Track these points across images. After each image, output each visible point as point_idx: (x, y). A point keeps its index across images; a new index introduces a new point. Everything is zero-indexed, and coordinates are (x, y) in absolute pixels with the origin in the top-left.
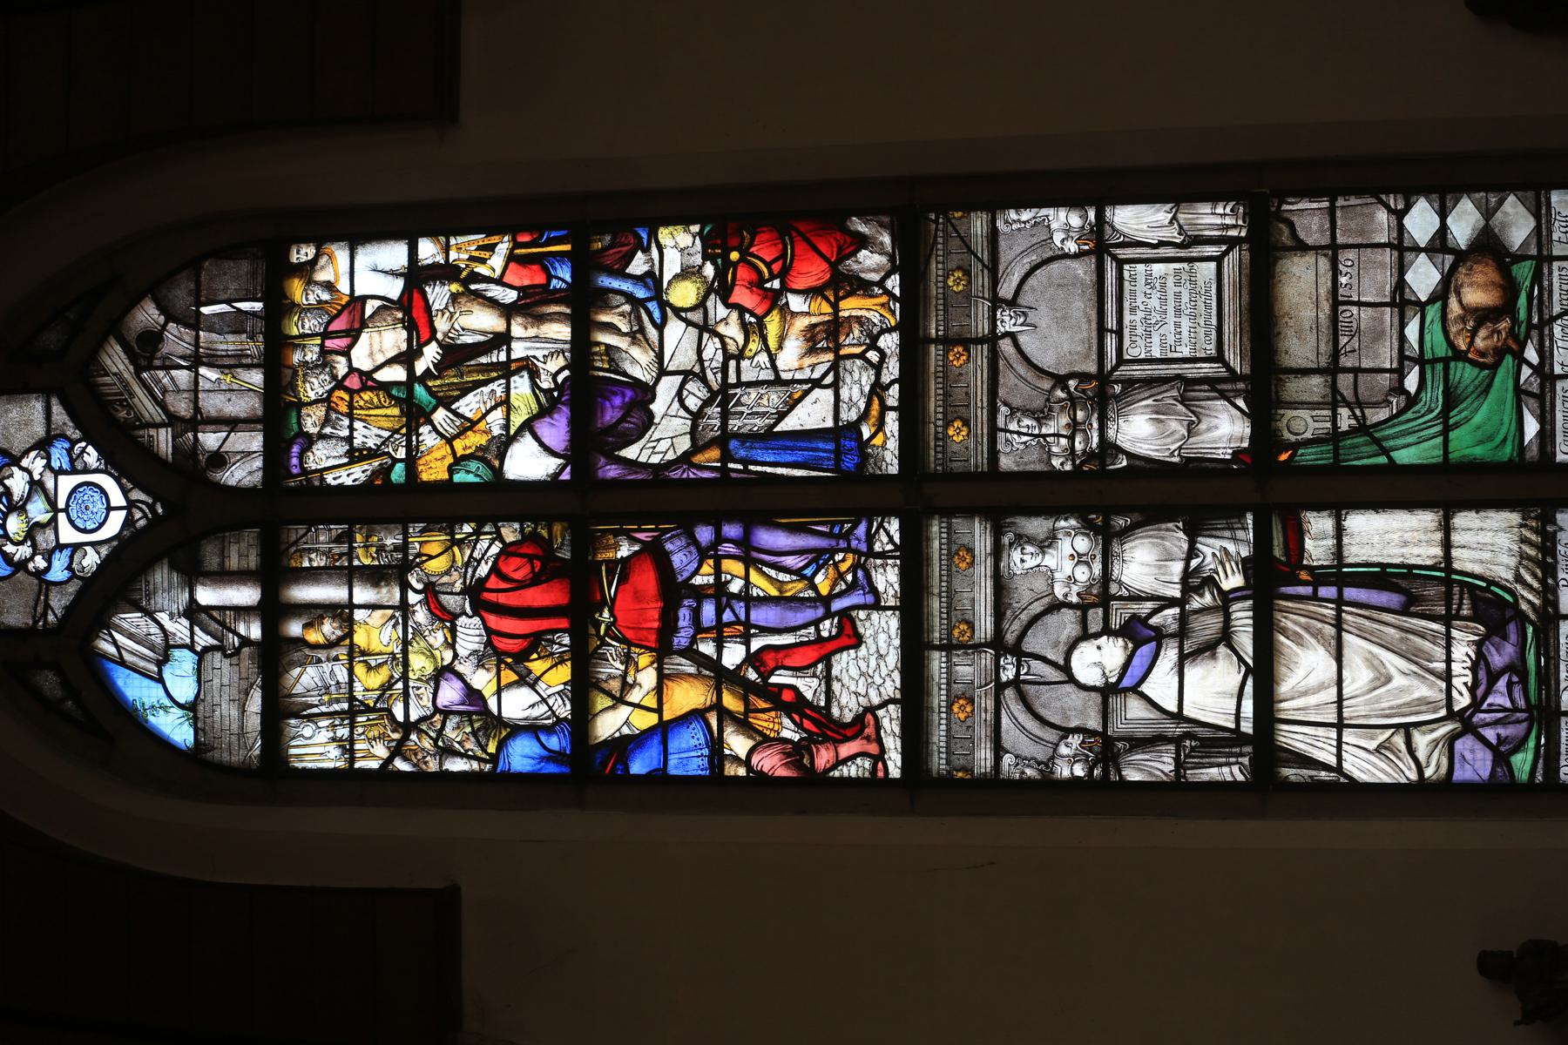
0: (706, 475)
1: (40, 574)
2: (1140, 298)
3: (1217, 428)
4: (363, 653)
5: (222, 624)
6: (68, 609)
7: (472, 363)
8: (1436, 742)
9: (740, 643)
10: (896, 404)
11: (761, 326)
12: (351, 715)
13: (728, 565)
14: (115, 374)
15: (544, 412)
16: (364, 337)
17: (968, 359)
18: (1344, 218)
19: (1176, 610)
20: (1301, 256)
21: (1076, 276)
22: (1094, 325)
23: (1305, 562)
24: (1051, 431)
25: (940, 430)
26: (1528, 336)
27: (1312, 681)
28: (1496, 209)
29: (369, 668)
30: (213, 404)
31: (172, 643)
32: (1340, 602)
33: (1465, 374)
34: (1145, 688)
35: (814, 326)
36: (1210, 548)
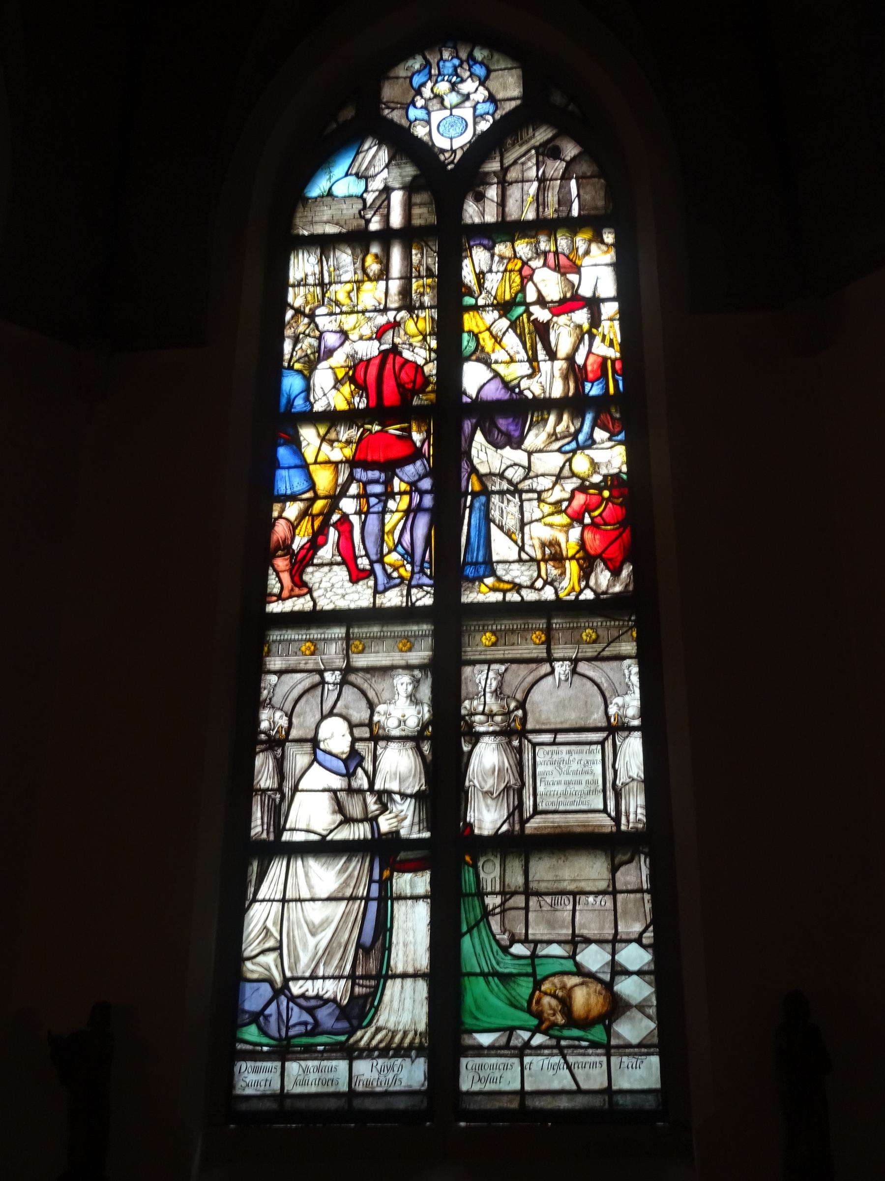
0: (464, 483)
1: (413, 103)
2: (577, 757)
3: (488, 811)
4: (358, 289)
5: (379, 207)
6: (392, 120)
7: (538, 339)
8: (268, 969)
9: (356, 509)
10: (507, 599)
11: (560, 512)
12: (321, 284)
13: (406, 499)
14: (534, 135)
15: (506, 384)
16: (556, 276)
17: (535, 644)
18: (635, 901)
19: (366, 786)
20: (607, 868)
21: (592, 713)
22: (559, 726)
23: (395, 874)
24: (488, 700)
25: (490, 628)
26: (551, 1037)
27: (314, 880)
28: (643, 1013)
29: (349, 293)
30: (514, 192)
31: (369, 180)
32: (367, 899)
33: (524, 987)
34: (316, 764)
35: (559, 545)
36: (406, 808)
